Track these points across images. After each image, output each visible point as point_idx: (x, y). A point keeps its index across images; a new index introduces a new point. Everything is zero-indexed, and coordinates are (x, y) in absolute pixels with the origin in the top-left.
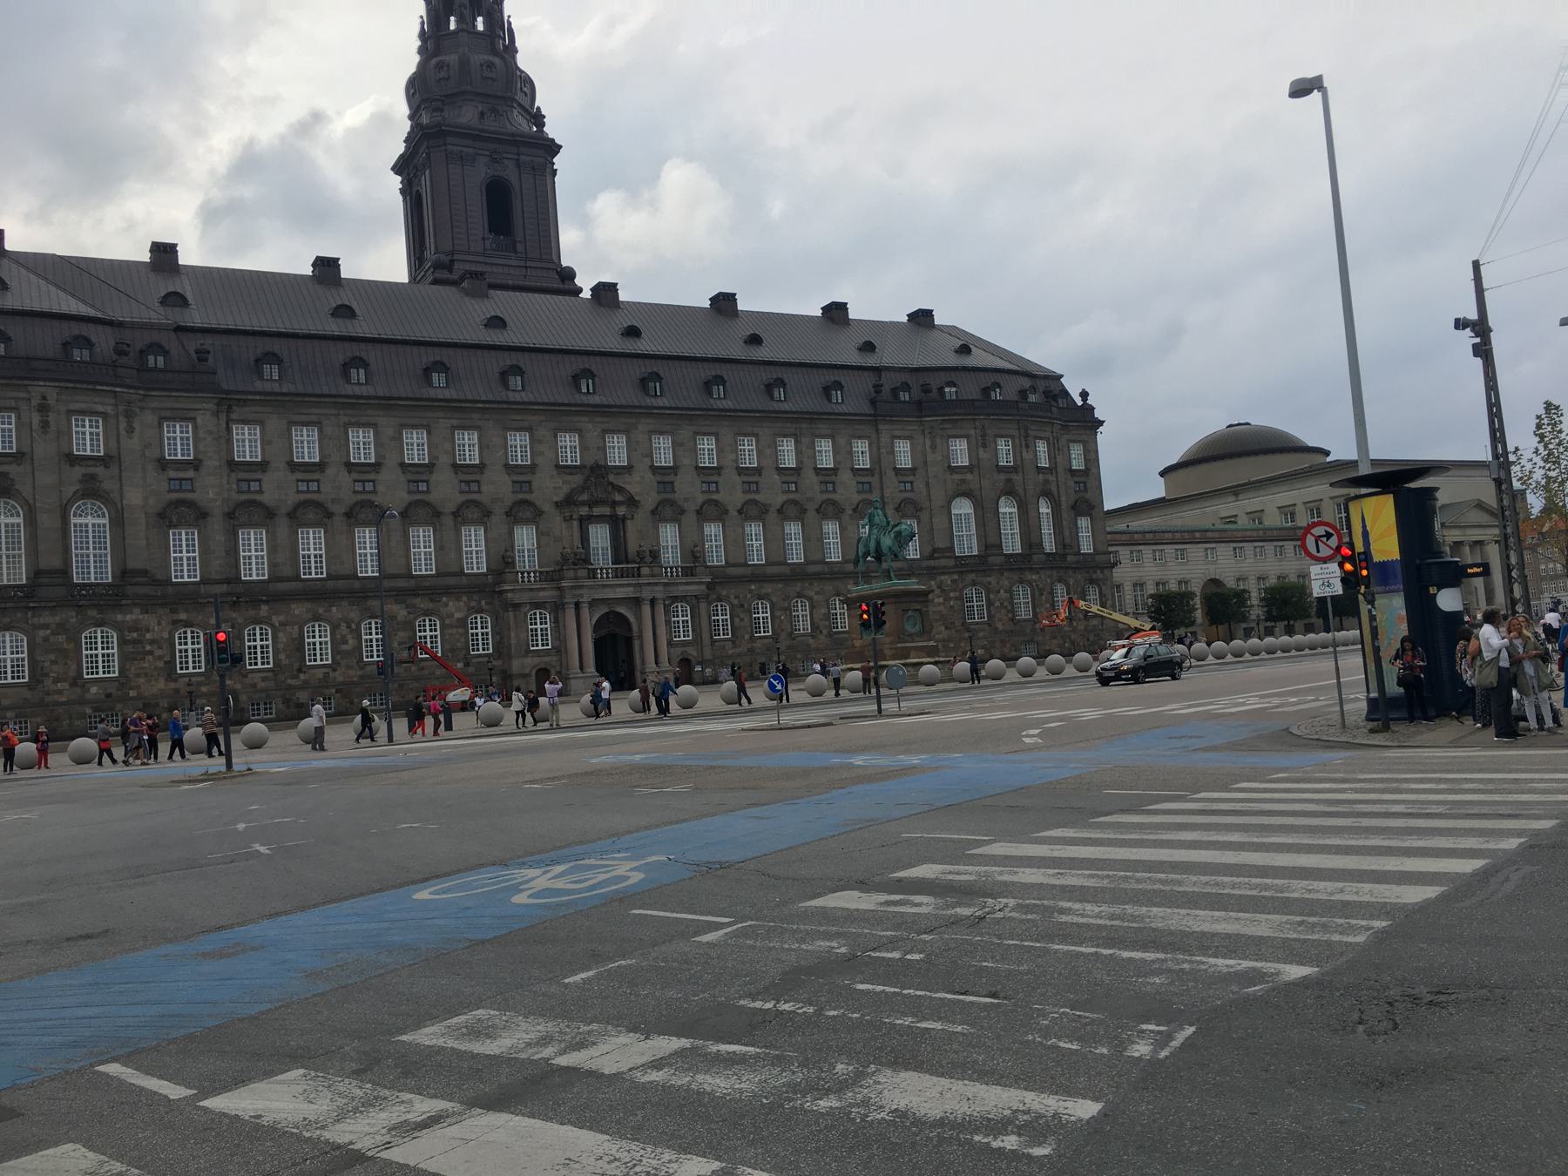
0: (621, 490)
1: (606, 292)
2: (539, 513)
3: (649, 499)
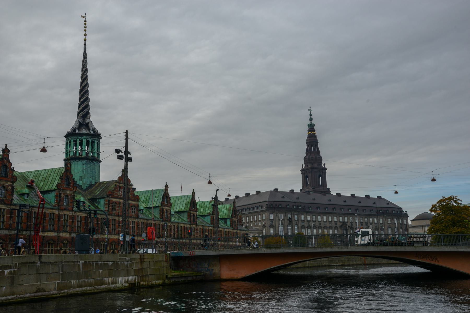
1: (338, 194)
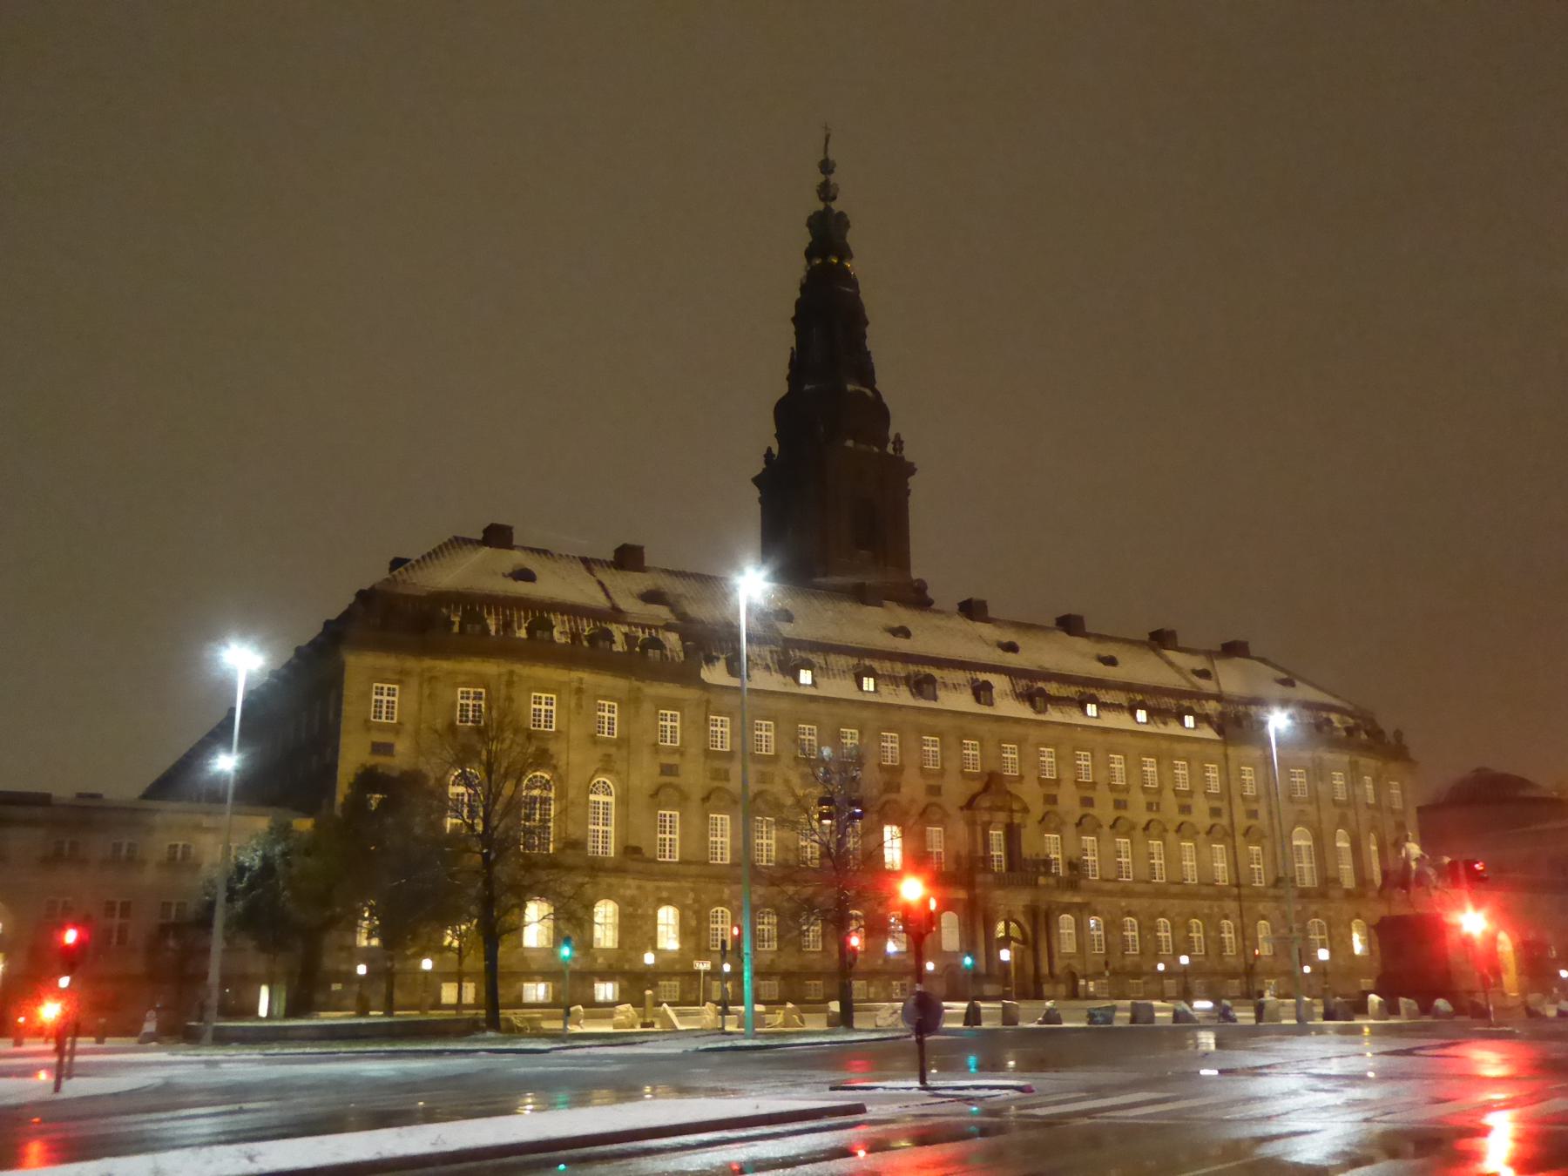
0: (1018, 798)
2: (946, 815)
3: (1038, 809)
